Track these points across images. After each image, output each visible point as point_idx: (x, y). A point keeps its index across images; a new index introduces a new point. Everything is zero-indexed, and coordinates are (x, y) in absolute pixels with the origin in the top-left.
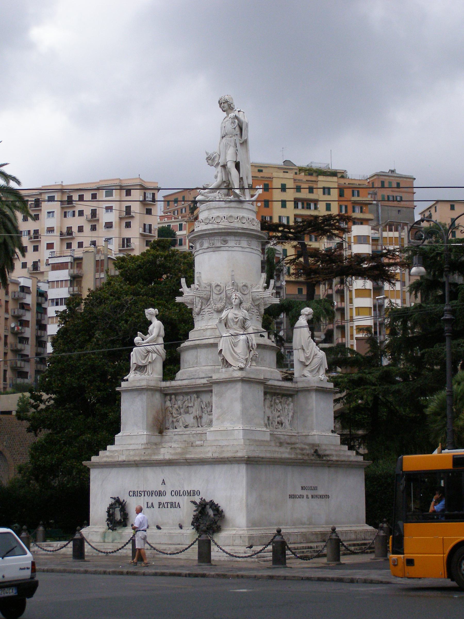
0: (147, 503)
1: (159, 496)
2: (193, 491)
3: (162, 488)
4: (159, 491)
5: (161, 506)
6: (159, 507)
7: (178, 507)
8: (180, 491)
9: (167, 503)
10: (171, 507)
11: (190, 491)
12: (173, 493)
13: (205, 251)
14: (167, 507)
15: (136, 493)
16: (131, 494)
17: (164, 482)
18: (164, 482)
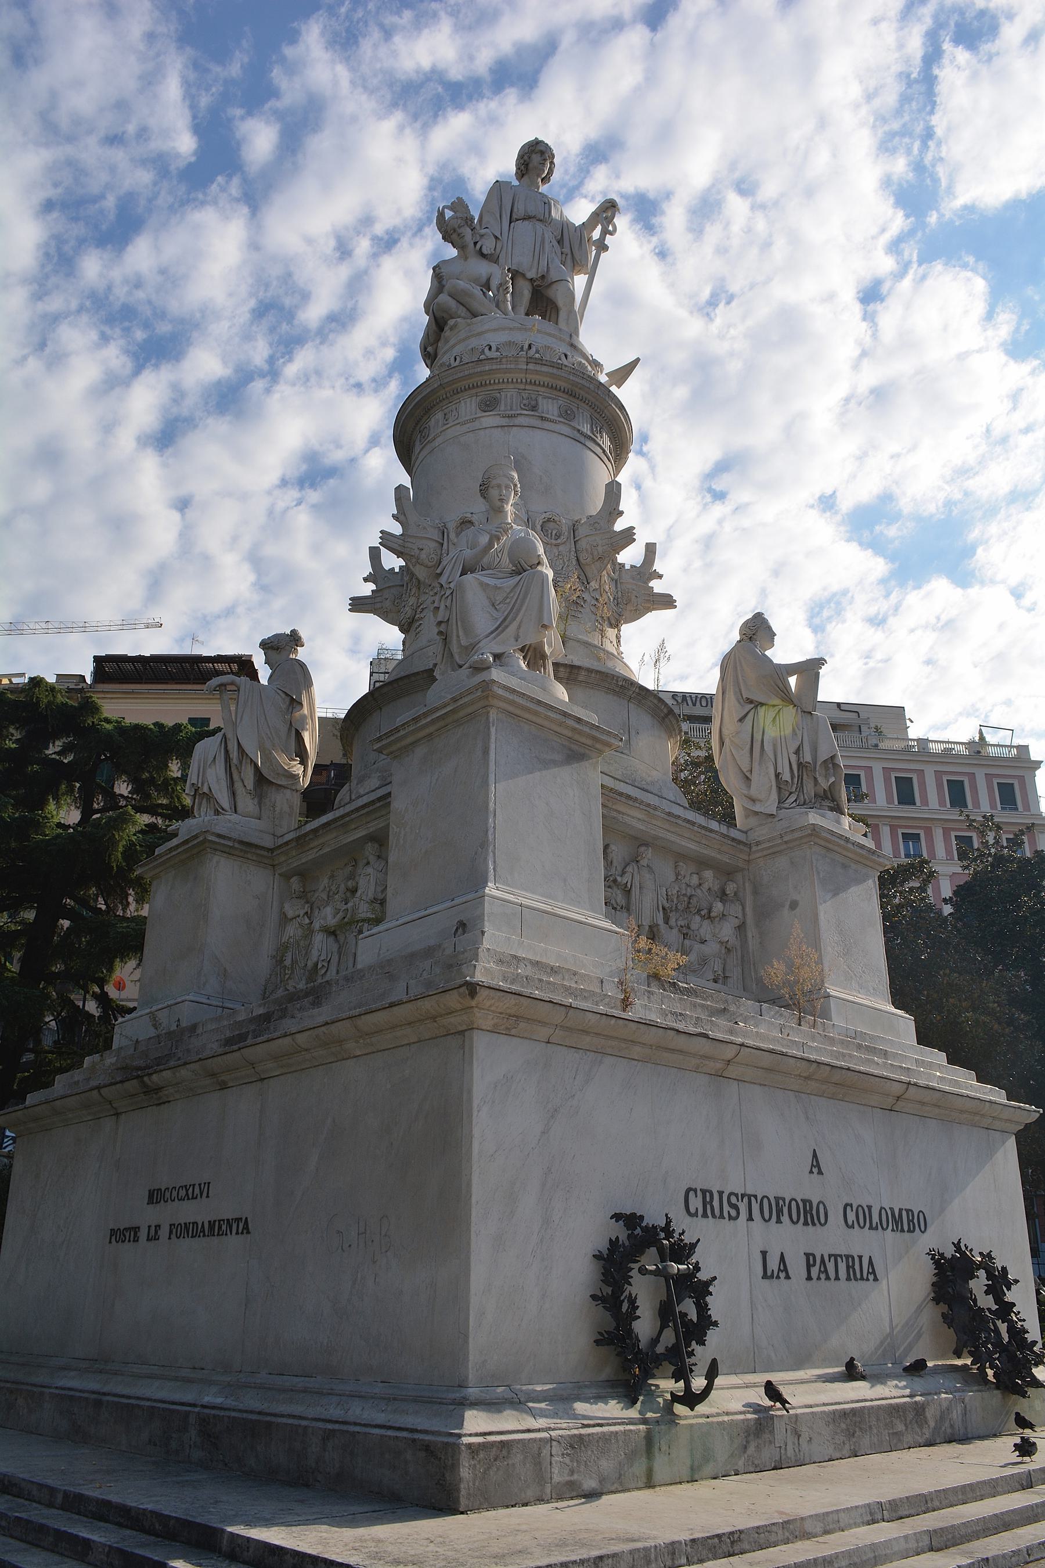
0: (764, 1254)
1: (806, 1224)
2: (907, 1211)
3: (810, 1189)
4: (804, 1201)
5: (815, 1271)
6: (809, 1278)
7: (871, 1277)
8: (870, 1208)
9: (836, 1256)
10: (848, 1279)
11: (901, 1210)
12: (851, 1217)
13: (582, 439)
14: (837, 1278)
15: (716, 1203)
16: (696, 1203)
17: (816, 1165)
18: (816, 1165)
